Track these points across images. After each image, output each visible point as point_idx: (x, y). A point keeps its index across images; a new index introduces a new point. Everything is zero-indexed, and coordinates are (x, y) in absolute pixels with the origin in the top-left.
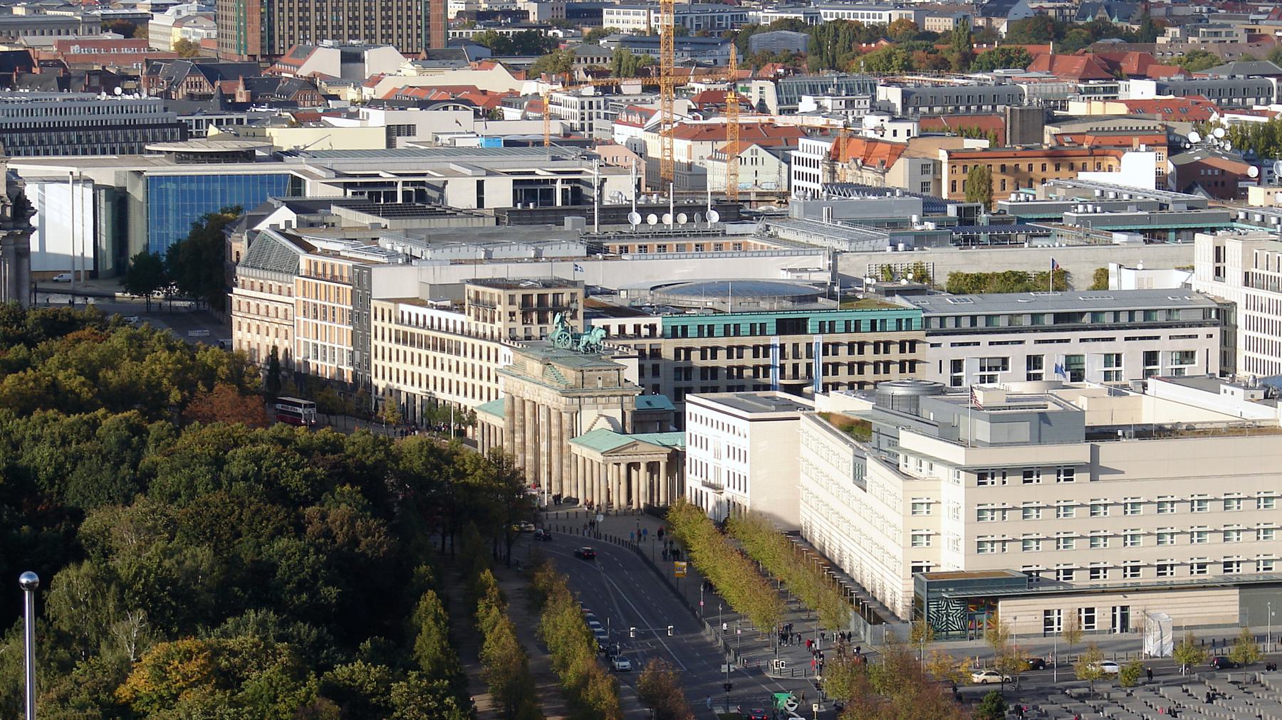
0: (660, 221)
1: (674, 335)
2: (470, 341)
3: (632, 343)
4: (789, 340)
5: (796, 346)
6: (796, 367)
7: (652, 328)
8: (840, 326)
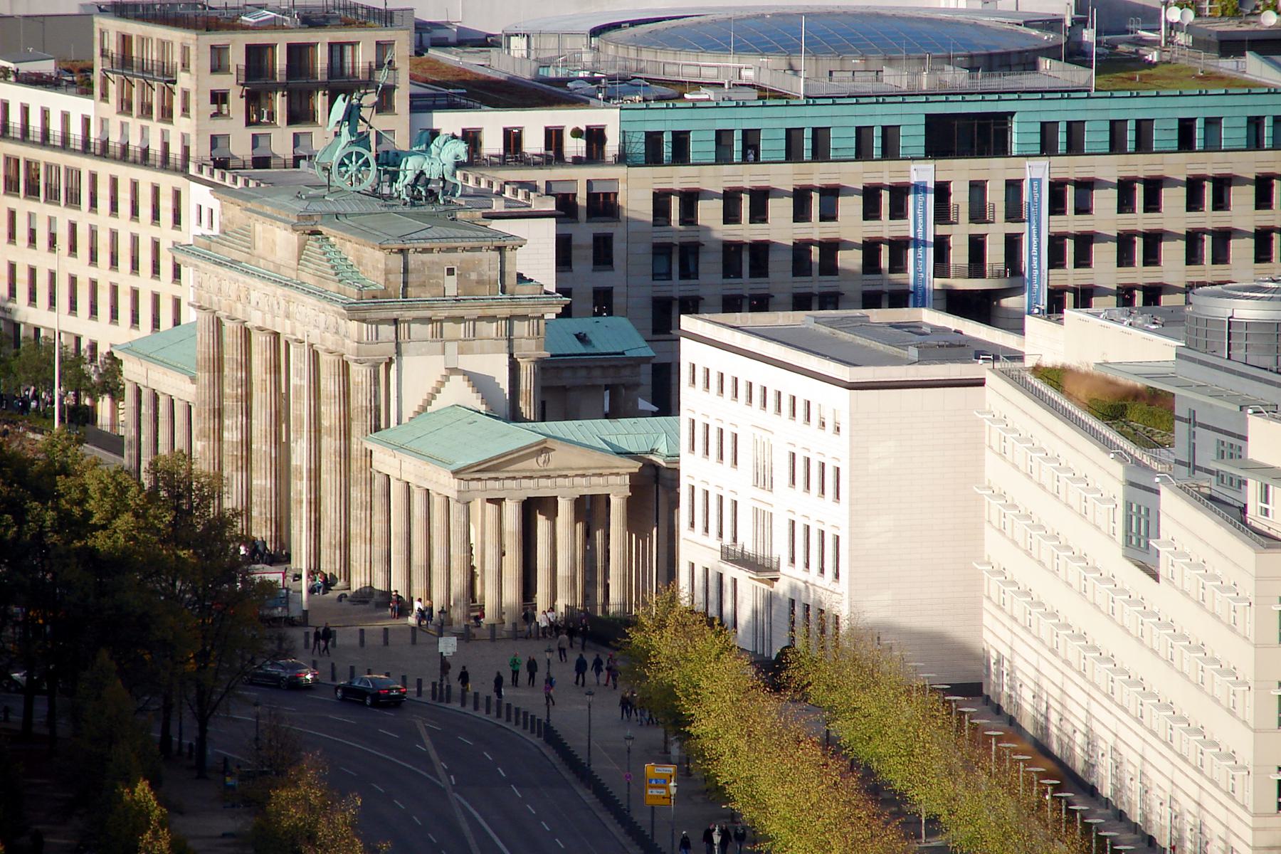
1: (653, 156)
2: (105, 169)
3: (540, 176)
4: (959, 172)
5: (977, 188)
6: (977, 246)
7: (595, 137)
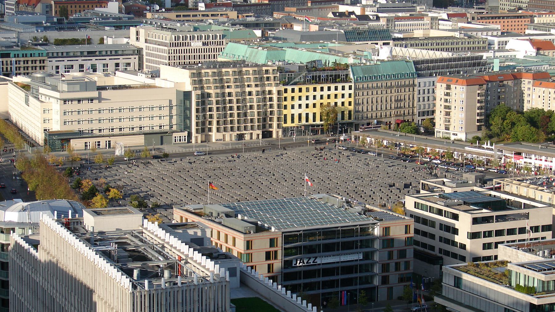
5: (7, 61)
6: (7, 68)
8: (21, 55)
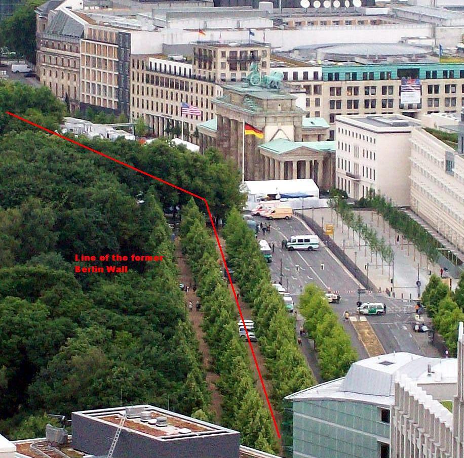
0: (322, 6)
1: (330, 79)
3: (302, 84)
8: (440, 74)
